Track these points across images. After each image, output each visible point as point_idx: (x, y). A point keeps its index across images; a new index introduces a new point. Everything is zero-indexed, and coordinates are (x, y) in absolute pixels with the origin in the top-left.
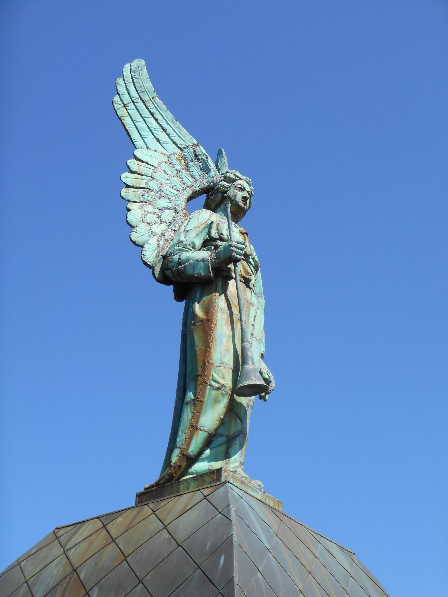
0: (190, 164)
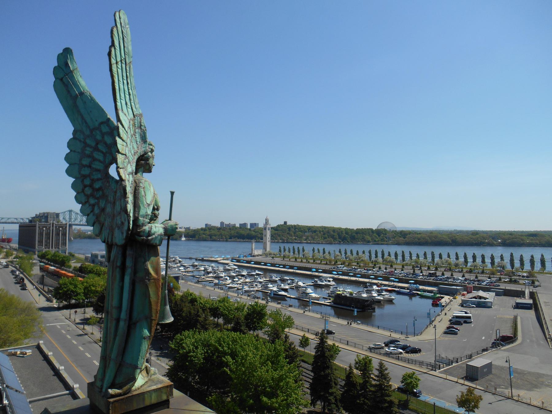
0: (137, 130)
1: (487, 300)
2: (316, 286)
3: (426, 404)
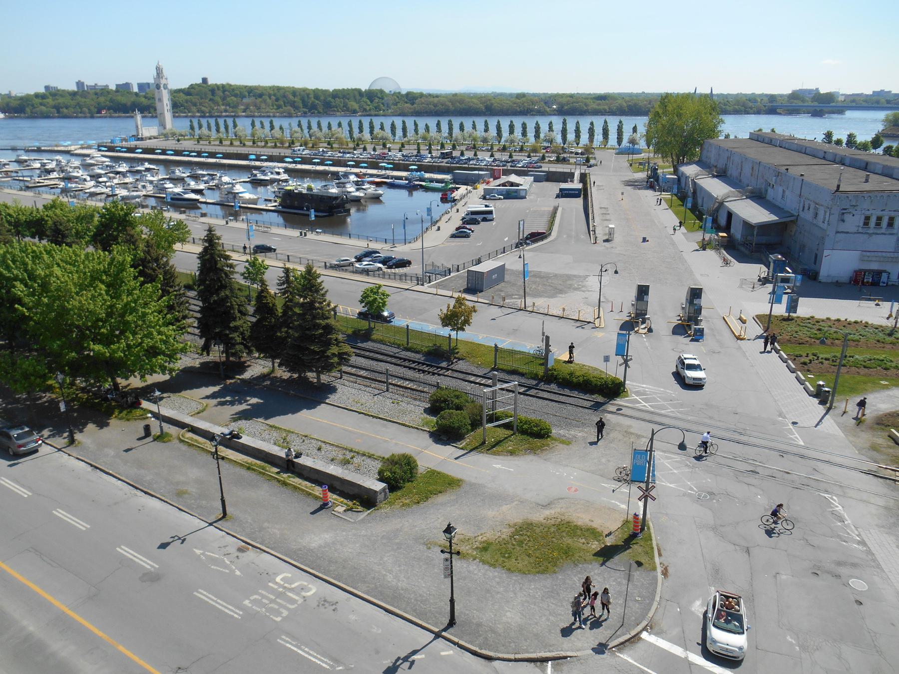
1: (520, 187)
2: (256, 183)
3: (398, 329)
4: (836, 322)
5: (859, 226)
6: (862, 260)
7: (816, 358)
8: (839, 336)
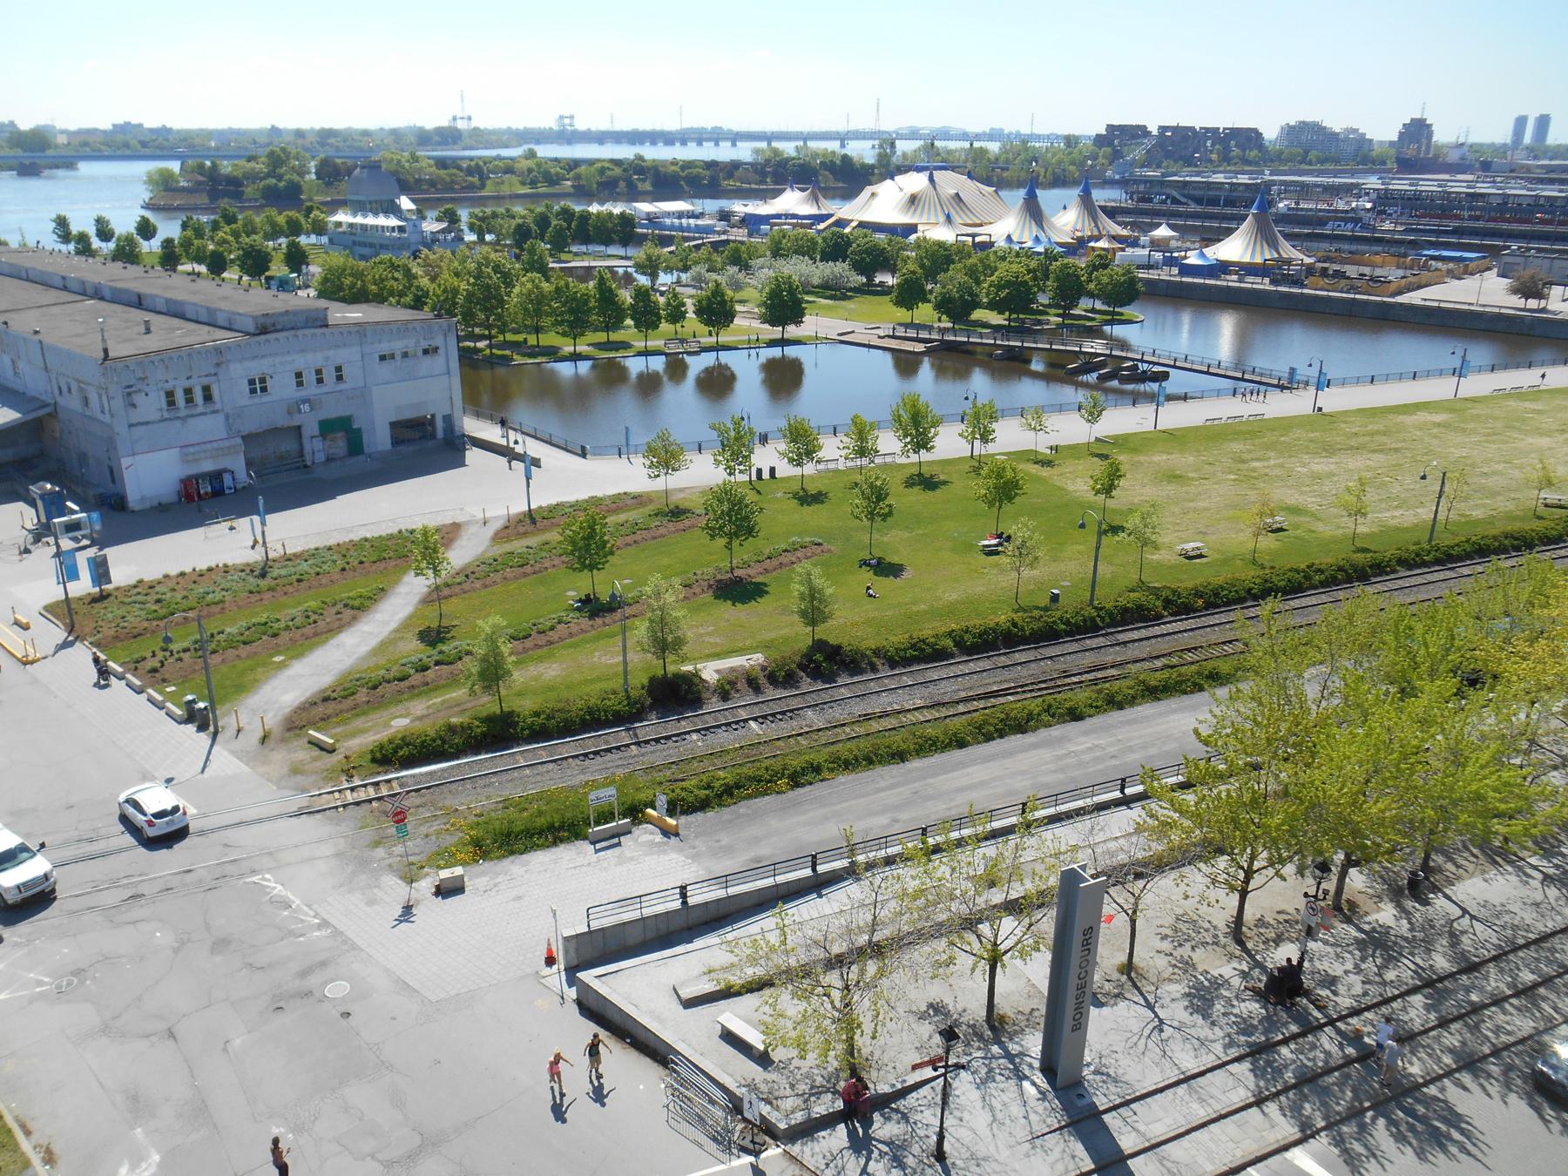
4: (180, 579)
5: (161, 409)
6: (185, 460)
7: (168, 654)
8: (192, 602)
